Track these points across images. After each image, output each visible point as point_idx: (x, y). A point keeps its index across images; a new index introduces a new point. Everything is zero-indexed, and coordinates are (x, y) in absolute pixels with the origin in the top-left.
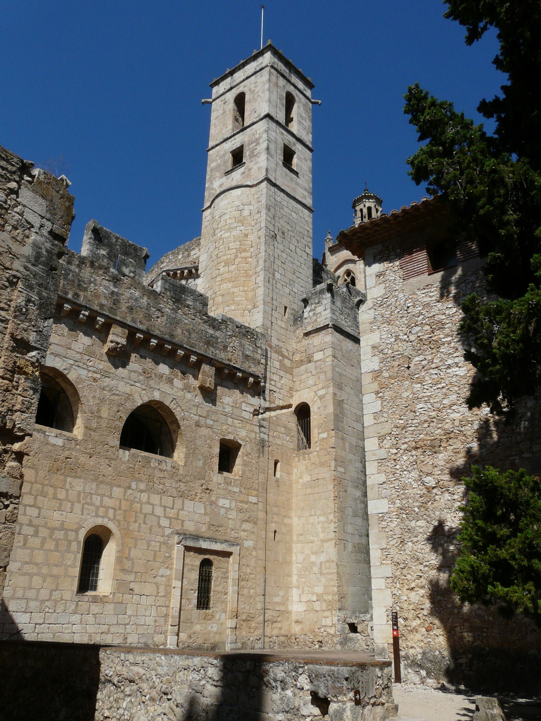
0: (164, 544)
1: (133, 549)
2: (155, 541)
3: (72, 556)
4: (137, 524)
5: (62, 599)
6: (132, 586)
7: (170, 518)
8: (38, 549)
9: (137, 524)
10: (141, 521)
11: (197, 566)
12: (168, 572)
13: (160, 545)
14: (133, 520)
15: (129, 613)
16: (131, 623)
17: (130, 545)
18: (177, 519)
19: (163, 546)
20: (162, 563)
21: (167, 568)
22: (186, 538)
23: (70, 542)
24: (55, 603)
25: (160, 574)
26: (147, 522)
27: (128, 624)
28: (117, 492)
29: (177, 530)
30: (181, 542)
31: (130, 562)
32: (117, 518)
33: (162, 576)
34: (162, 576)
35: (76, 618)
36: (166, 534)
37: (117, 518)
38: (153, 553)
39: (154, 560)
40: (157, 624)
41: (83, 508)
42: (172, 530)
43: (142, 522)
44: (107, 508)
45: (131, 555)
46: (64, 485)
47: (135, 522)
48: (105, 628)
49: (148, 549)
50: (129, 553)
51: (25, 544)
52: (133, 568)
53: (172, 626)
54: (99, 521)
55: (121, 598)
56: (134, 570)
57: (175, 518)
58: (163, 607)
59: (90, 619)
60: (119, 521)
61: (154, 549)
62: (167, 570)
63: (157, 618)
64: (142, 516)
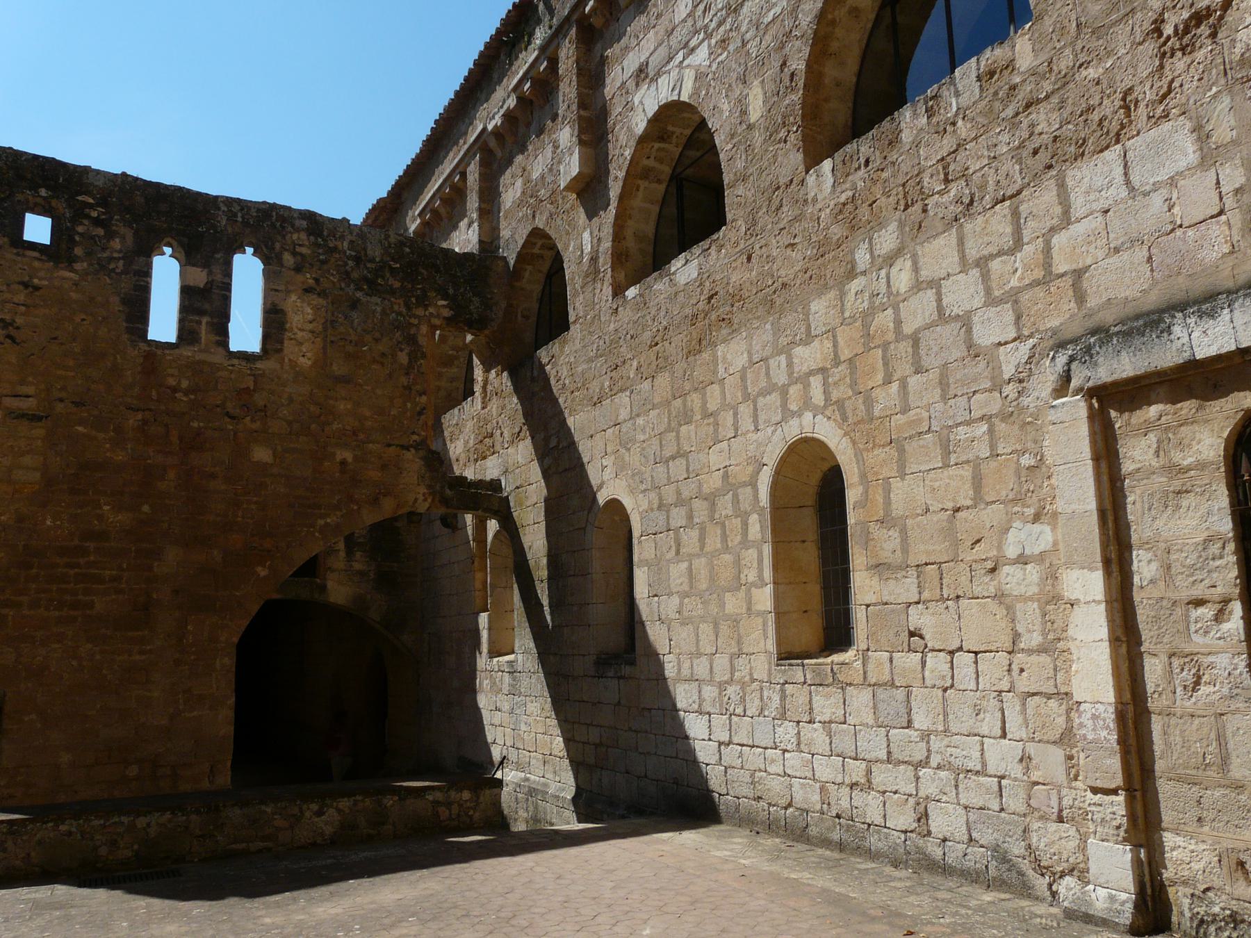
0: (1006, 417)
1: (896, 484)
2: (968, 423)
3: (752, 554)
4: (895, 386)
5: (753, 680)
6: (916, 618)
7: (1013, 297)
8: (698, 556)
9: (895, 386)
10: (903, 368)
11: (1201, 466)
12: (1041, 537)
13: (991, 431)
14: (880, 377)
15: (921, 721)
16: (935, 761)
17: (885, 472)
18: (1048, 277)
19: (1001, 427)
20: (1015, 501)
21: (1037, 518)
22: (1088, 350)
23: (744, 517)
24: (742, 689)
25: (1011, 552)
26: (926, 362)
27: (924, 763)
28: (820, 308)
29: (1055, 332)
30: (1066, 377)
31: (894, 533)
32: (835, 395)
33: (1022, 560)
34: (1022, 560)
35: (786, 732)
36: (1008, 371)
37: (835, 395)
38: (967, 472)
39: (978, 499)
40: (1036, 776)
41: (756, 410)
42: (1031, 342)
43: (907, 369)
44: (804, 380)
45: (894, 506)
46: (715, 372)
47: (888, 381)
48: (857, 771)
49: (946, 466)
50: (888, 502)
51: (678, 552)
52: (905, 549)
53: (1095, 791)
54: (793, 430)
55: (887, 671)
56: (913, 561)
57: (1036, 283)
58: (1049, 697)
59: (816, 735)
60: (840, 404)
61: (971, 456)
62: (1037, 527)
63: (1032, 748)
64: (905, 348)
